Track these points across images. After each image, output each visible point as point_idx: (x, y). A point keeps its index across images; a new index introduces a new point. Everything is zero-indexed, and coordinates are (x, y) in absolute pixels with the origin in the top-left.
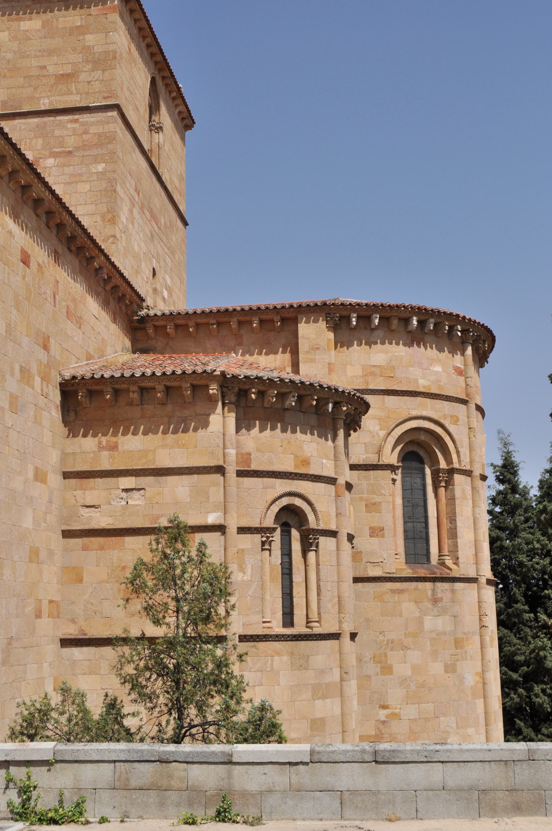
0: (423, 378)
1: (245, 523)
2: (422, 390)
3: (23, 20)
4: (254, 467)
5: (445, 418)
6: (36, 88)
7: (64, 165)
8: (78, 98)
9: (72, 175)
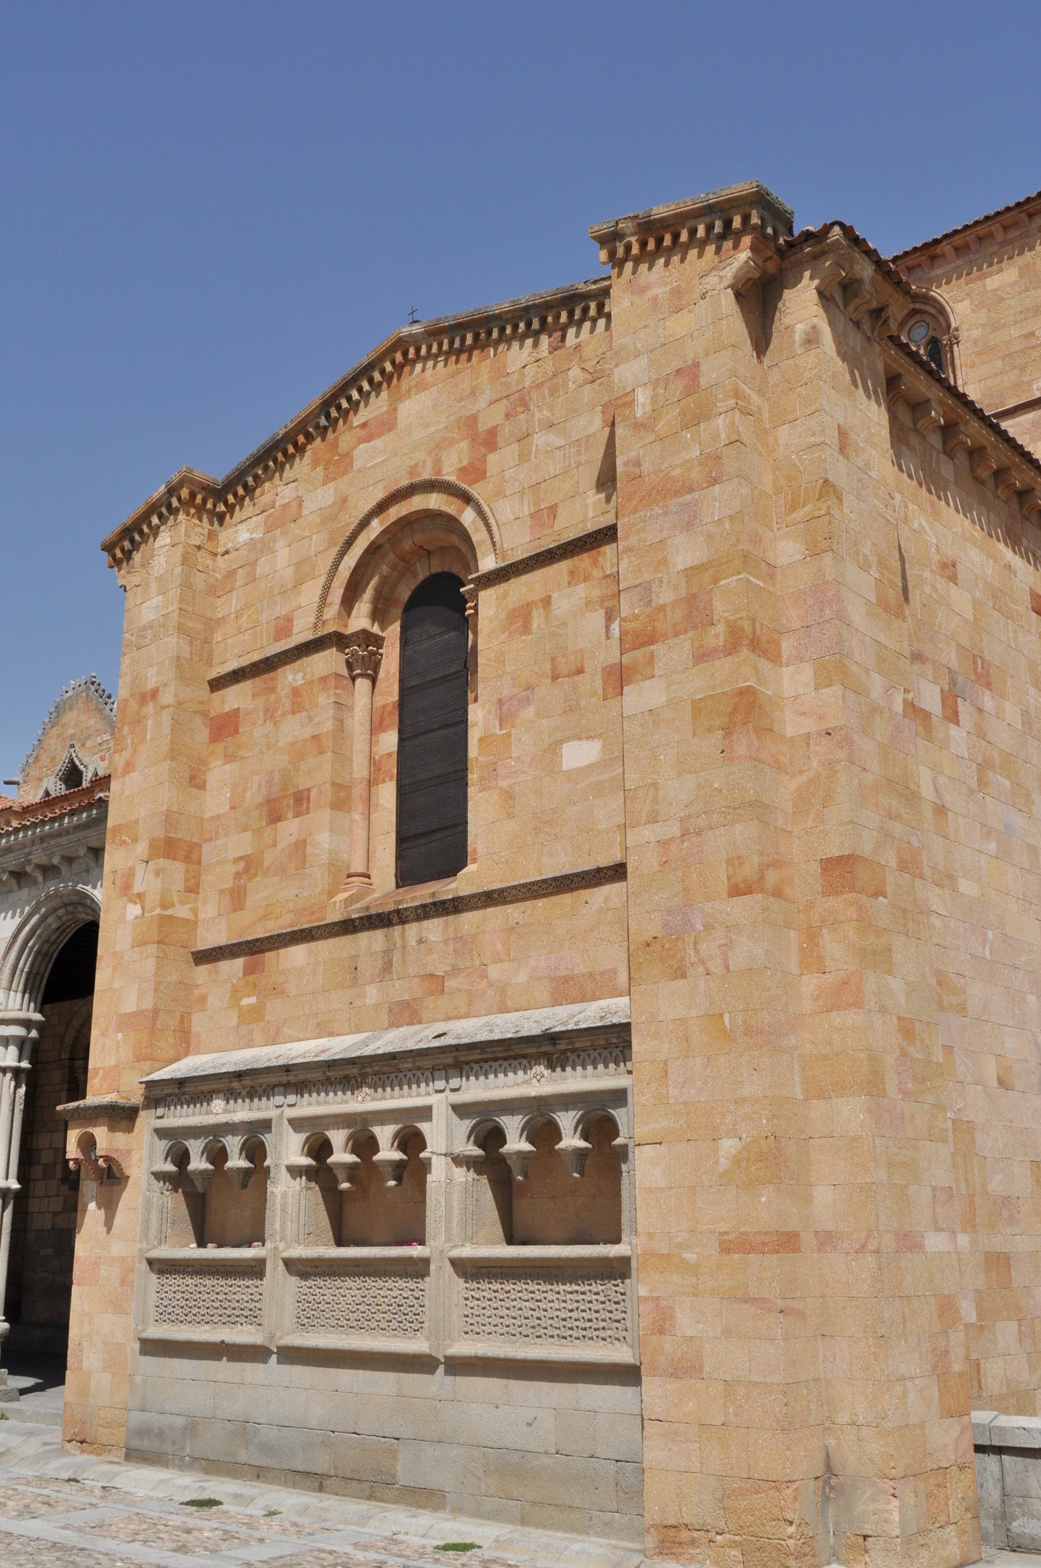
3: (991, 275)
6: (1023, 369)
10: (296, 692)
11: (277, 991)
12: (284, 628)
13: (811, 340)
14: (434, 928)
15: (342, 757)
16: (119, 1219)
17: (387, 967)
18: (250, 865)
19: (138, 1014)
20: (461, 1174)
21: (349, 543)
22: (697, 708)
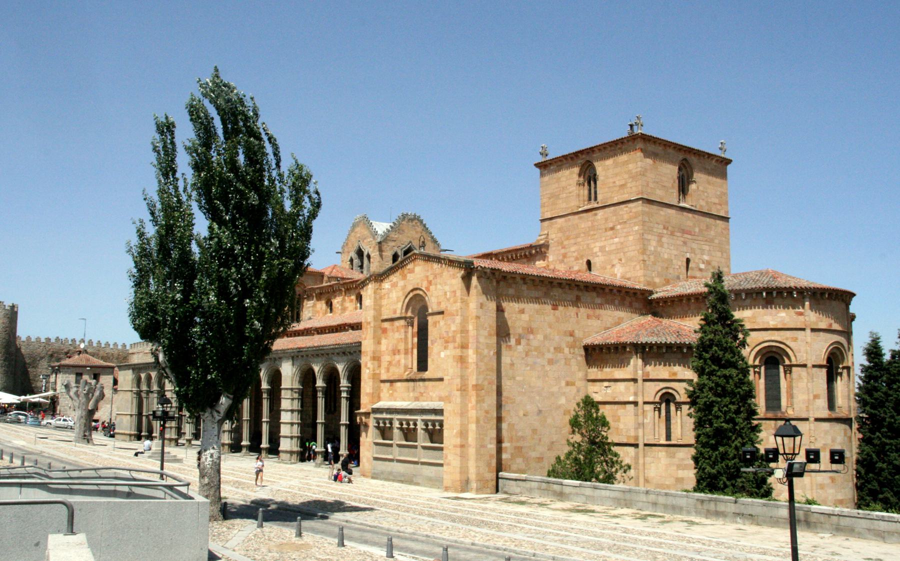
0: (773, 320)
1: (647, 400)
2: (772, 327)
4: (651, 377)
5: (787, 339)
7: (625, 228)
8: (627, 195)
9: (626, 233)
10: (397, 327)
11: (396, 391)
12: (395, 312)
13: (476, 287)
14: (421, 383)
15: (406, 343)
16: (369, 434)
17: (414, 390)
18: (390, 363)
19: (369, 393)
20: (422, 431)
21: (406, 297)
22: (454, 357)
